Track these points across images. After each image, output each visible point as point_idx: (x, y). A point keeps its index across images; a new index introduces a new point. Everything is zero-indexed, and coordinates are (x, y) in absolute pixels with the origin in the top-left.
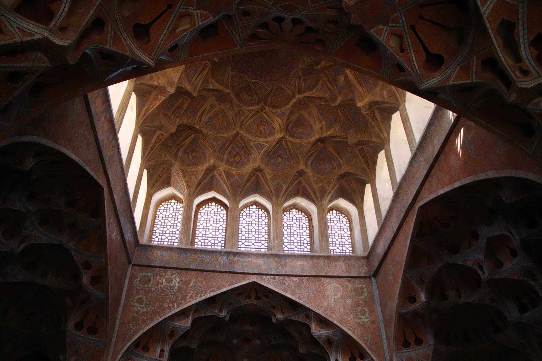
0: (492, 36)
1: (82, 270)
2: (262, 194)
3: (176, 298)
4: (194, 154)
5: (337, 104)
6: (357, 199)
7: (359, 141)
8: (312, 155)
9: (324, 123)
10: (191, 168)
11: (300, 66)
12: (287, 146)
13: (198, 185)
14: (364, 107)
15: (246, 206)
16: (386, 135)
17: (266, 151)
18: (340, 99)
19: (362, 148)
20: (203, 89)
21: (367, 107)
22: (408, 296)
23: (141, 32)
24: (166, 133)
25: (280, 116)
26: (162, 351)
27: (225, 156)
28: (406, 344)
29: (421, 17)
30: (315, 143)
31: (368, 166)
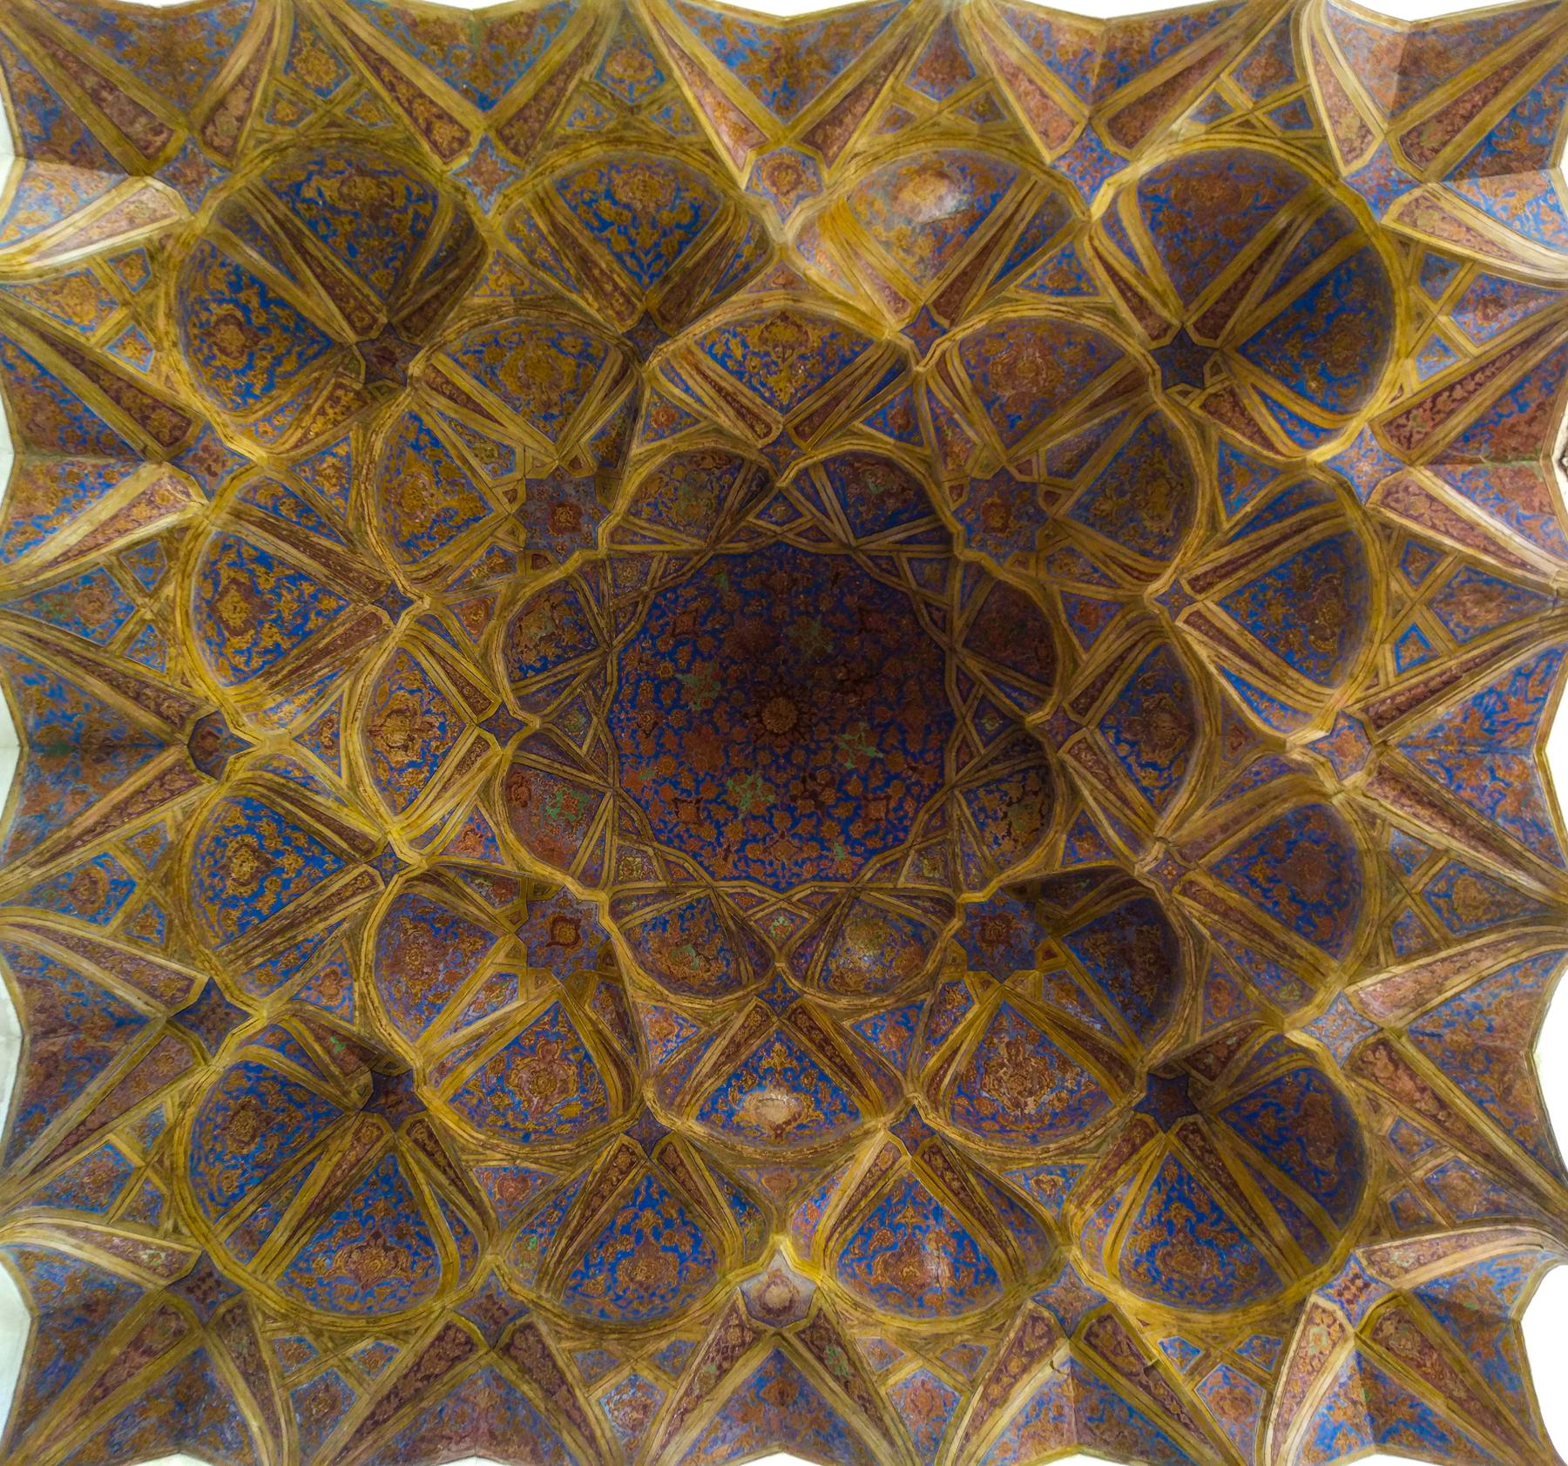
4: (230, 336)
5: (663, 1122)
7: (523, 1311)
8: (299, 1053)
10: (168, 315)
11: (726, 887)
12: (340, 898)
13: (73, 353)
14: (777, 1278)
17: (308, 781)
18: (691, 1126)
19: (470, 1344)
20: (632, 411)
21: (776, 1295)
24: (475, 169)
25: (475, 827)
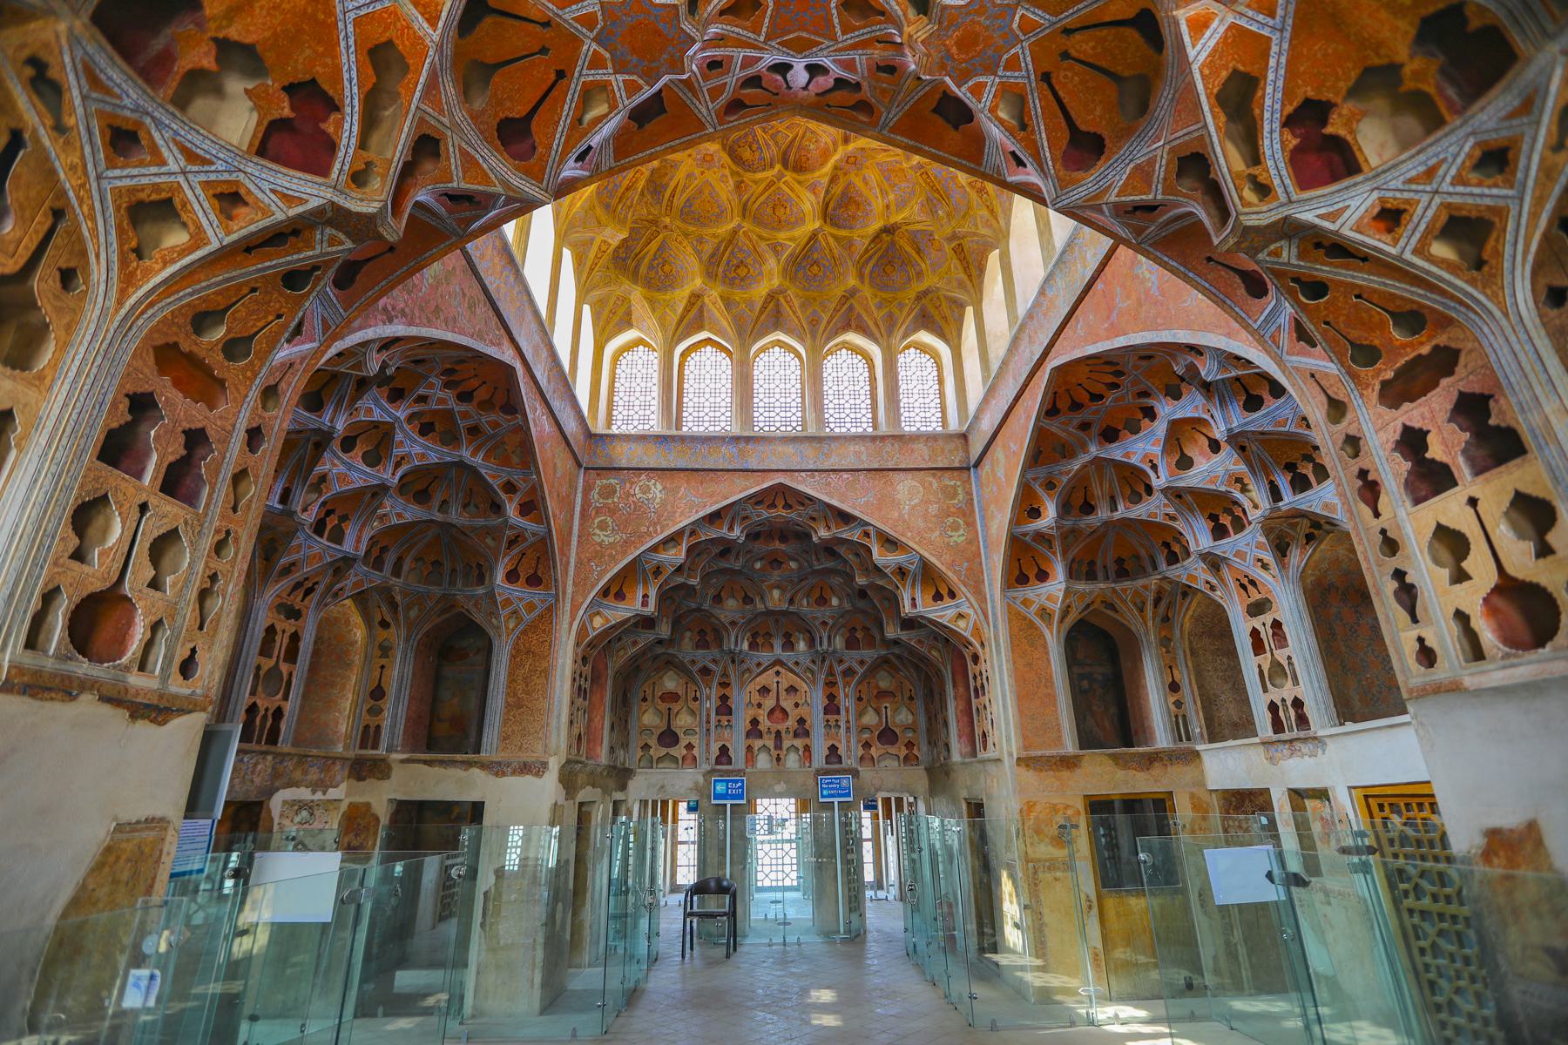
0: (1206, 108)
1: (503, 496)
2: (788, 332)
3: (659, 517)
4: (667, 268)
6: (948, 329)
9: (891, 197)
13: (680, 321)
15: (763, 350)
16: (1002, 222)
17: (791, 255)
22: (1028, 508)
23: (514, 135)
25: (813, 188)
26: (645, 596)
27: (721, 269)
28: (1022, 580)
29: (1065, 55)
30: (876, 238)
31: (970, 276)
